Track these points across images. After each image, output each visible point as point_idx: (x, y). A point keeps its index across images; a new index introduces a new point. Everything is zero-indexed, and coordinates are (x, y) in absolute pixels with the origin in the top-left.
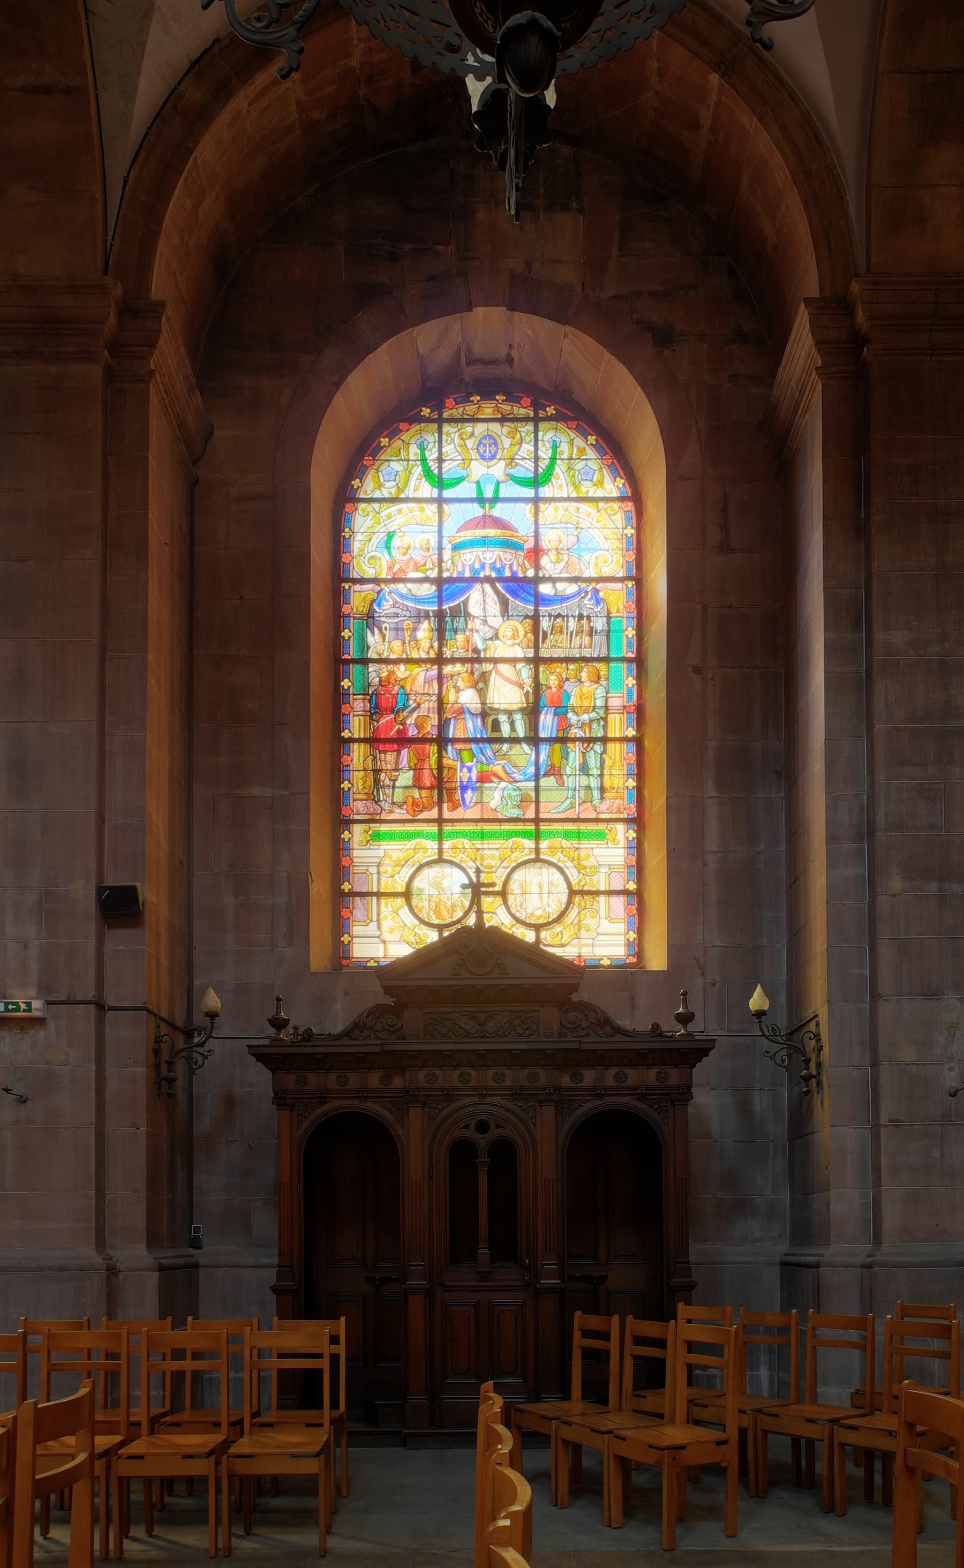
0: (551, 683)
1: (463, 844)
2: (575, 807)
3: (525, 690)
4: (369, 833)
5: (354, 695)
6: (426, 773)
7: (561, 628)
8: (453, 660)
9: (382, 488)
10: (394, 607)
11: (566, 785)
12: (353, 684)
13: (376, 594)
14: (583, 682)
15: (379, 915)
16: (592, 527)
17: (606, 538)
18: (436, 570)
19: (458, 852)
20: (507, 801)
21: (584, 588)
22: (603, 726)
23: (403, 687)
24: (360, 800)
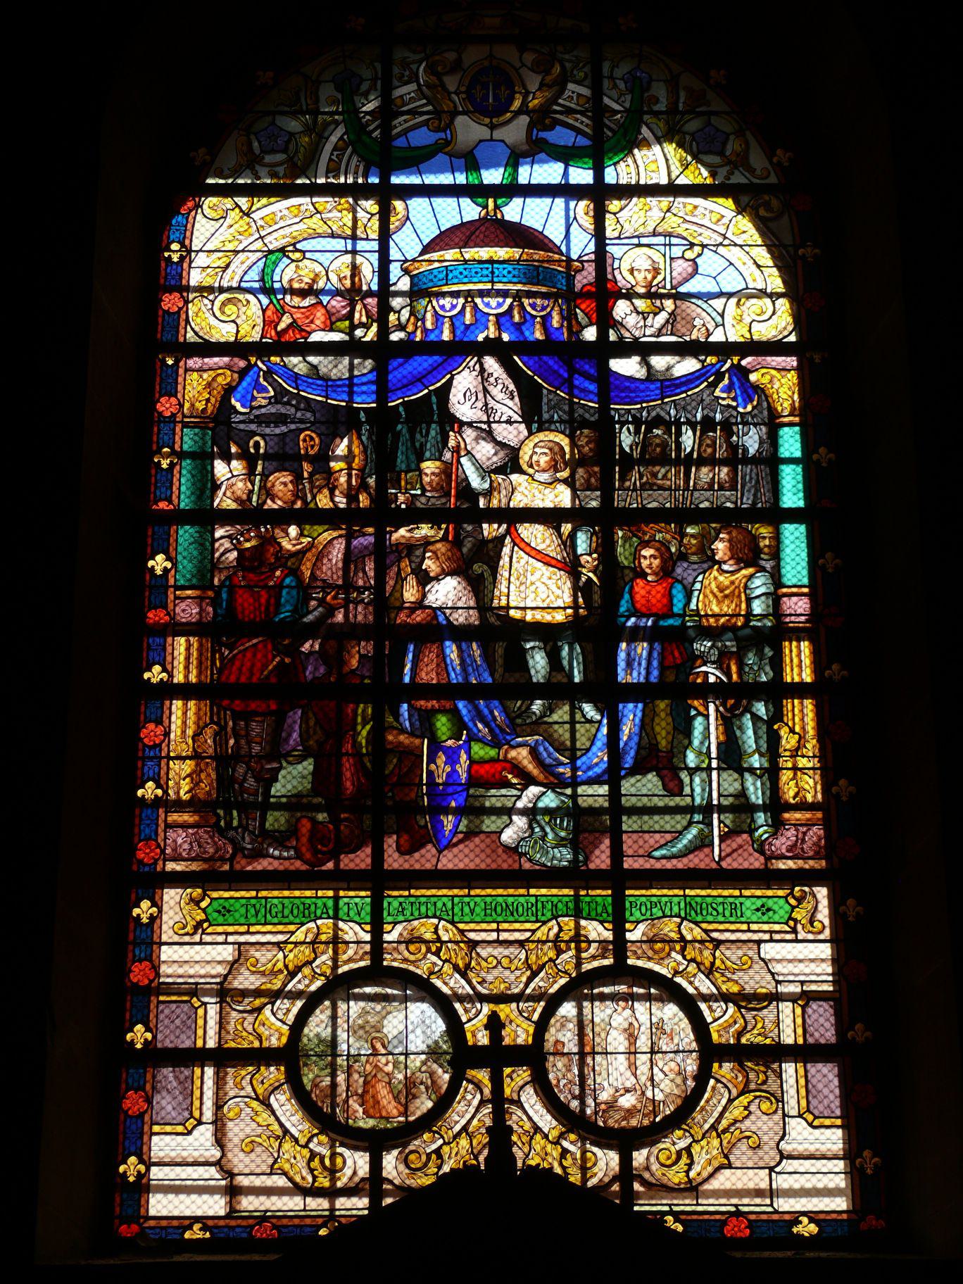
0: (645, 563)
1: (436, 932)
2: (712, 844)
3: (584, 579)
4: (203, 905)
5: (177, 588)
6: (347, 765)
7: (664, 445)
8: (413, 516)
9: (257, 167)
10: (277, 402)
11: (687, 790)
12: (175, 565)
13: (236, 376)
14: (719, 563)
15: (218, 1106)
16: (726, 242)
17: (759, 266)
18: (374, 328)
19: (424, 949)
20: (543, 829)
21: (713, 365)
22: (771, 659)
23: (296, 573)
24: (184, 826)
